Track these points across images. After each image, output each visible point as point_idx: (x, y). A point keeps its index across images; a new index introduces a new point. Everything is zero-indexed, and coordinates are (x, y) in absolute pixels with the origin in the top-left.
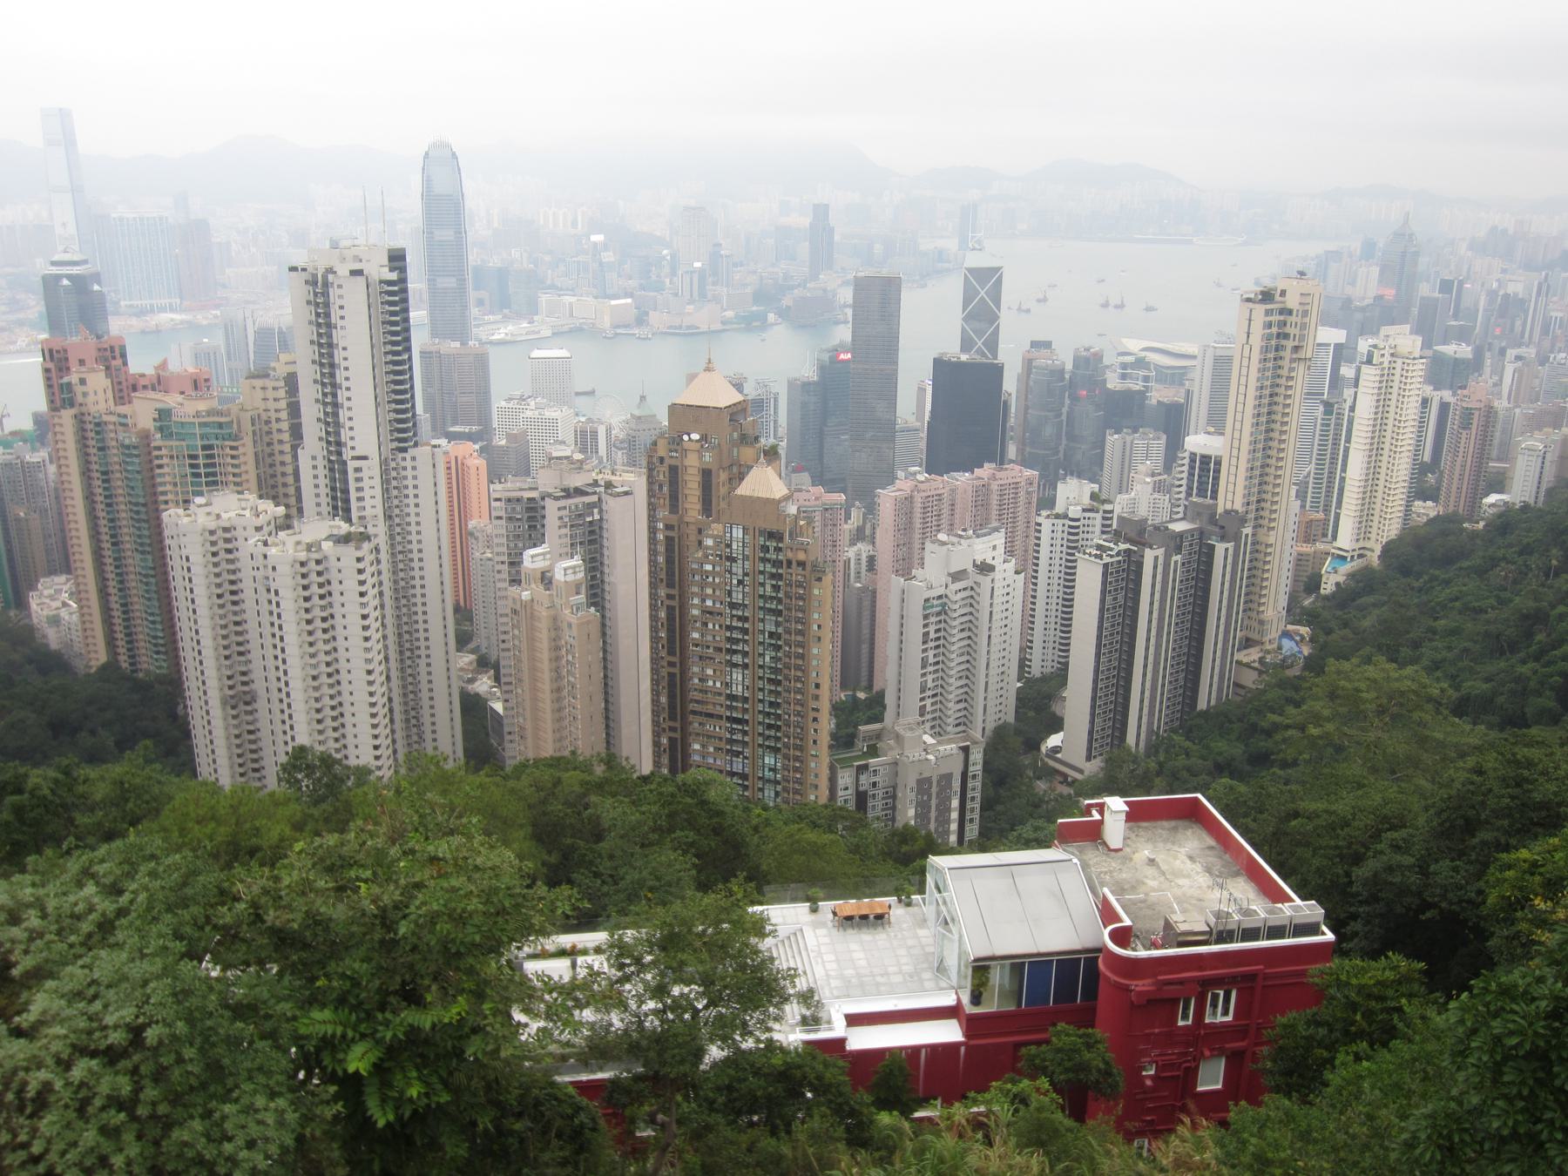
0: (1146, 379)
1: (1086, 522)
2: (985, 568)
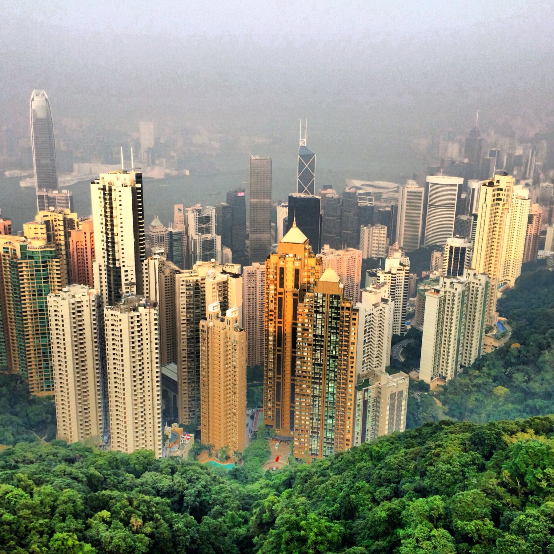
0: (370, 200)
1: (399, 275)
2: (384, 301)
